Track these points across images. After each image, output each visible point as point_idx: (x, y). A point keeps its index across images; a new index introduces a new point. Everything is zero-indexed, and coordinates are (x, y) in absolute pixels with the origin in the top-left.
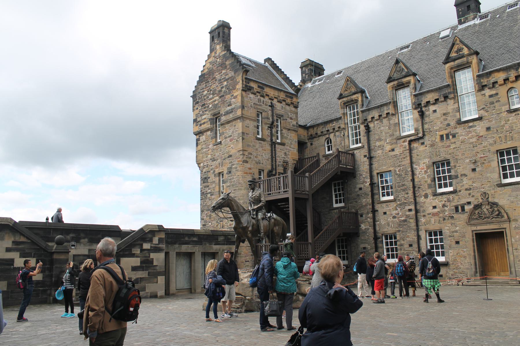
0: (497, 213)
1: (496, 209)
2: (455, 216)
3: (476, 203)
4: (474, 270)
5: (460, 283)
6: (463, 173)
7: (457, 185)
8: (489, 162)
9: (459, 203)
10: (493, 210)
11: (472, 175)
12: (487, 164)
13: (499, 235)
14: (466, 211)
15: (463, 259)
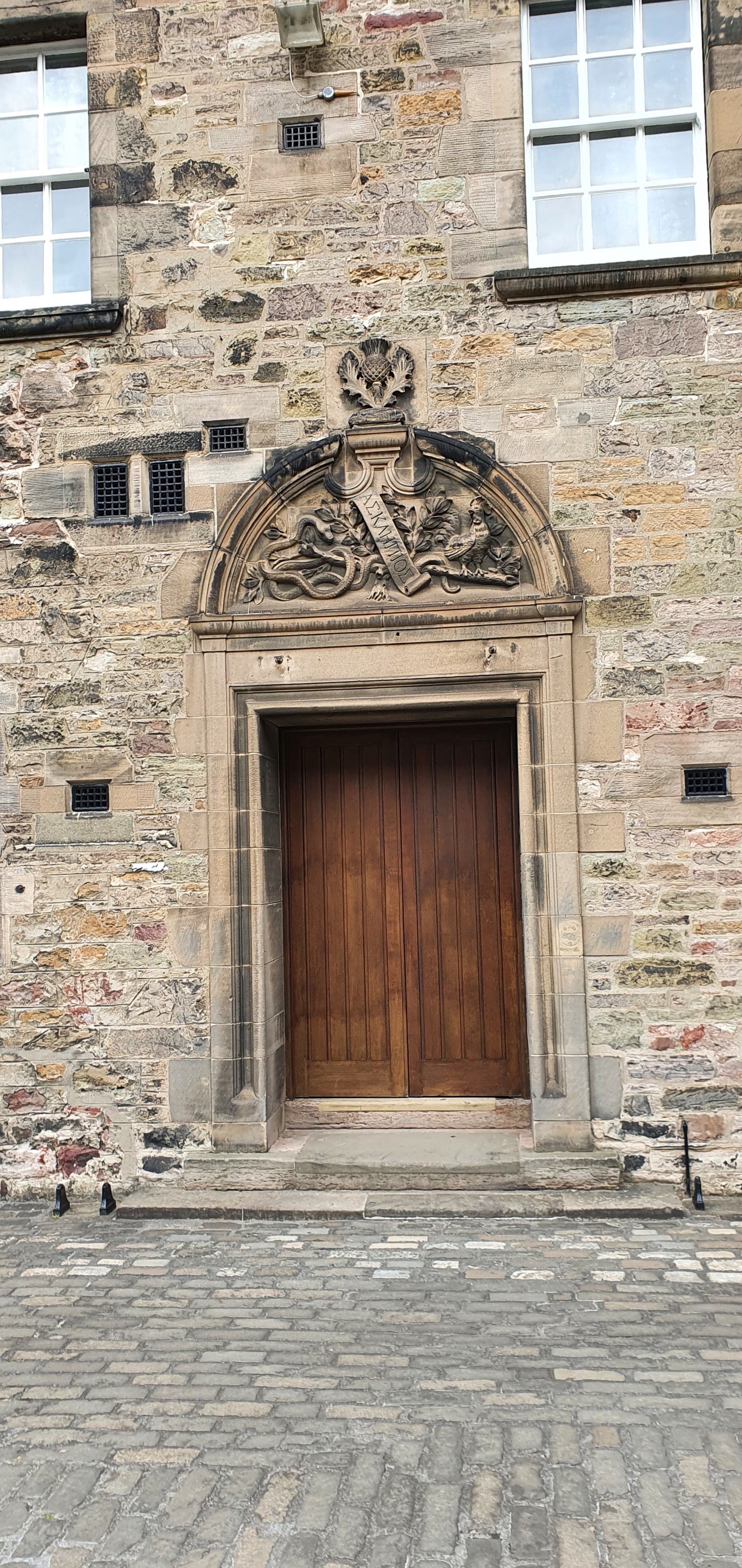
0: (477, 533)
1: (465, 501)
2: (89, 544)
3: (293, 435)
4: (219, 1052)
5: (85, 1180)
6: (197, 153)
7: (135, 259)
8: (447, 69)
9: (135, 430)
10: (439, 515)
11: (284, 176)
12: (421, 88)
13: (469, 748)
14: (192, 505)
15: (125, 944)
